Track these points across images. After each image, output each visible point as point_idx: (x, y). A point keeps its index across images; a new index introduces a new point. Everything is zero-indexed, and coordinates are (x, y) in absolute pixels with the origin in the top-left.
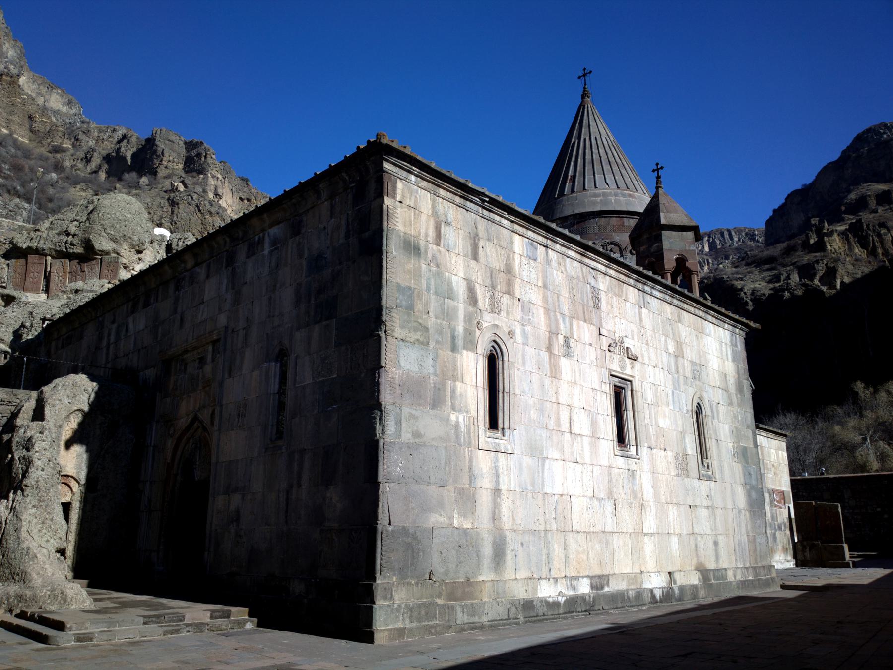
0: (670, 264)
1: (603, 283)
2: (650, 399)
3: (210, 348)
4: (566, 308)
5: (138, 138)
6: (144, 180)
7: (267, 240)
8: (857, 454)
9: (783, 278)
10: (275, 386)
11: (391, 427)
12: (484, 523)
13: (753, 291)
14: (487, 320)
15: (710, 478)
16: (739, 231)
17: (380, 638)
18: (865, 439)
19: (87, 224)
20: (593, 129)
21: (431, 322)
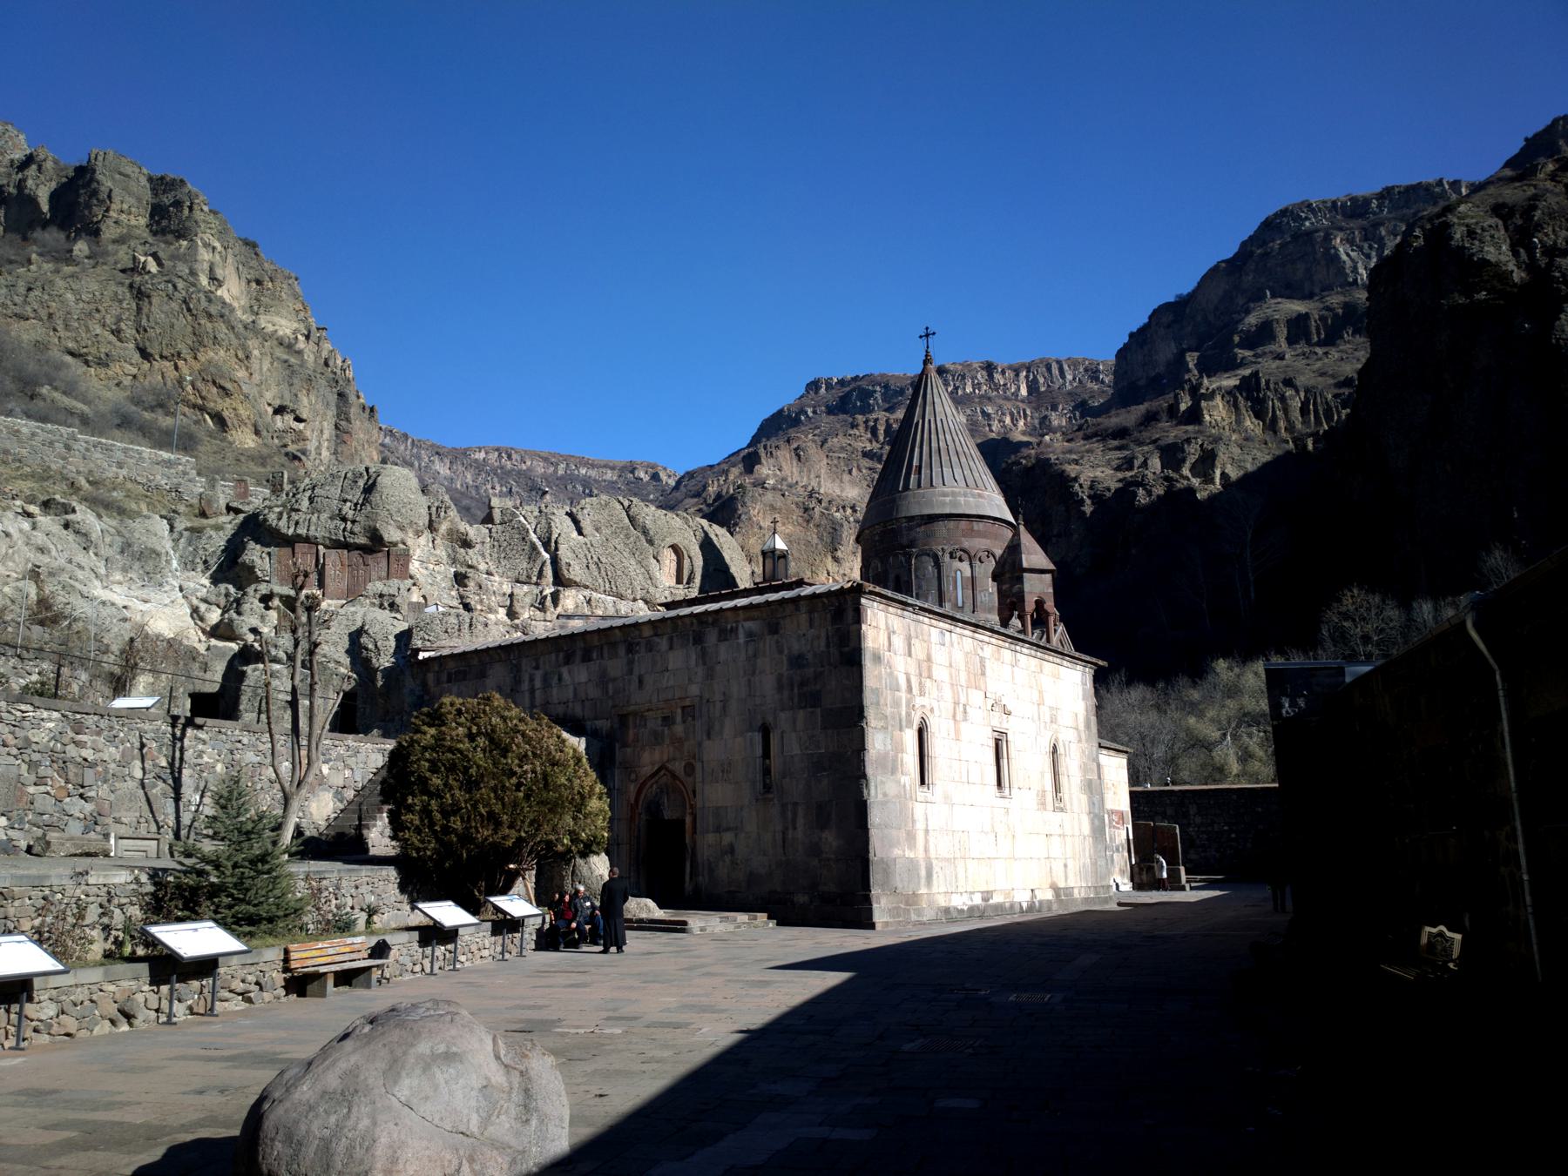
0: (1030, 606)
1: (988, 651)
5: (56, 162)
6: (81, 248)
7: (741, 631)
9: (1137, 463)
10: (759, 751)
11: (873, 792)
12: (920, 854)
14: (919, 701)
15: (1062, 810)
16: (1074, 364)
17: (878, 927)
18: (1225, 735)
20: (939, 408)
21: (889, 711)
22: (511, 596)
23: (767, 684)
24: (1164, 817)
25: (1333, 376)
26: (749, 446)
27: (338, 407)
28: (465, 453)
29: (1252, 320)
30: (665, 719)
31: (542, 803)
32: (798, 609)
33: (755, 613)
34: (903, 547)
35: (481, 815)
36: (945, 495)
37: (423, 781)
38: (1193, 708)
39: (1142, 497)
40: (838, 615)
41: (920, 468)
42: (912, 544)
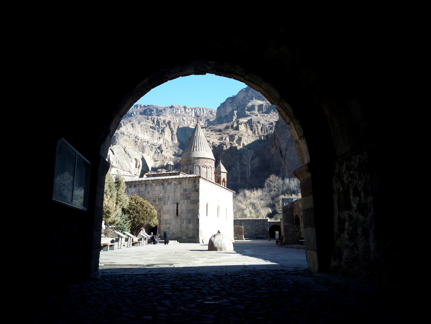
0: (222, 180)
9: (224, 139)
10: (176, 208)
16: (207, 110)
23: (178, 194)
24: (237, 225)
25: (268, 122)
29: (250, 104)
30: (154, 201)
33: (176, 180)
34: (192, 164)
37: (128, 212)
38: (240, 201)
39: (225, 148)
40: (195, 181)
42: (194, 163)
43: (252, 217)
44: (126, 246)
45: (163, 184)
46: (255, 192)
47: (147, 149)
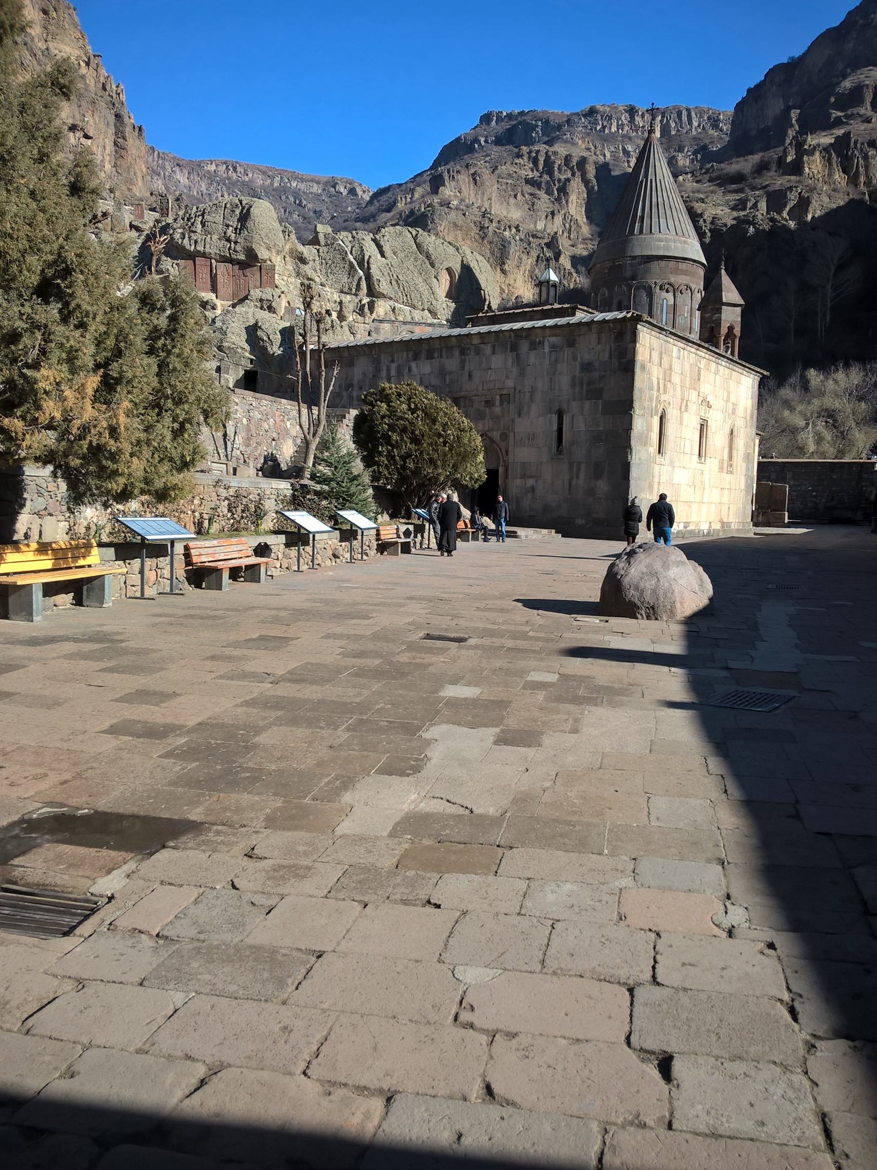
0: (724, 331)
2: (713, 429)
3: (498, 397)
4: (688, 383)
7: (546, 343)
8: (799, 438)
9: (749, 205)
10: (555, 427)
13: (714, 218)
14: (663, 397)
15: (731, 473)
16: (700, 112)
18: (808, 424)
19: (246, 232)
20: (658, 171)
21: (646, 404)
22: (341, 303)
23: (564, 381)
24: (769, 479)
26: (431, 168)
27: (116, 126)
28: (200, 165)
30: (487, 402)
31: (459, 454)
32: (590, 330)
33: (558, 331)
34: (626, 279)
35: (424, 459)
36: (660, 240)
37: (387, 438)
38: (787, 404)
40: (620, 336)
41: (642, 218)
42: (633, 278)
43: (823, 455)
44: (348, 555)
45: (514, 348)
46: (840, 375)
47: (514, 250)
